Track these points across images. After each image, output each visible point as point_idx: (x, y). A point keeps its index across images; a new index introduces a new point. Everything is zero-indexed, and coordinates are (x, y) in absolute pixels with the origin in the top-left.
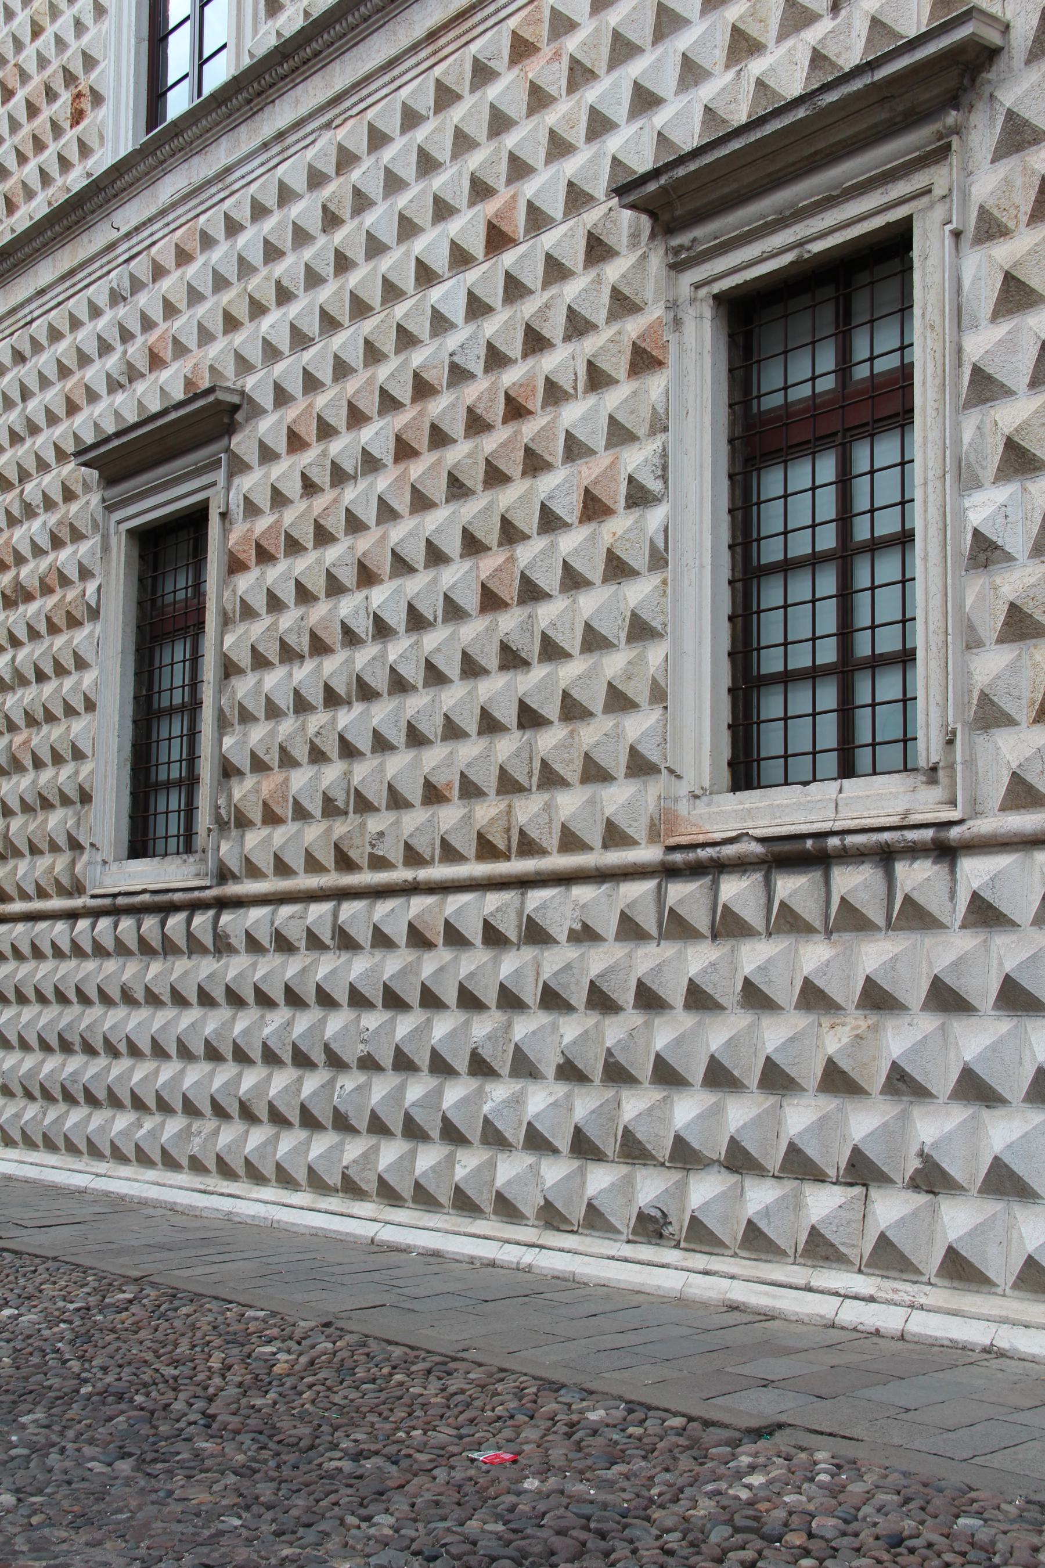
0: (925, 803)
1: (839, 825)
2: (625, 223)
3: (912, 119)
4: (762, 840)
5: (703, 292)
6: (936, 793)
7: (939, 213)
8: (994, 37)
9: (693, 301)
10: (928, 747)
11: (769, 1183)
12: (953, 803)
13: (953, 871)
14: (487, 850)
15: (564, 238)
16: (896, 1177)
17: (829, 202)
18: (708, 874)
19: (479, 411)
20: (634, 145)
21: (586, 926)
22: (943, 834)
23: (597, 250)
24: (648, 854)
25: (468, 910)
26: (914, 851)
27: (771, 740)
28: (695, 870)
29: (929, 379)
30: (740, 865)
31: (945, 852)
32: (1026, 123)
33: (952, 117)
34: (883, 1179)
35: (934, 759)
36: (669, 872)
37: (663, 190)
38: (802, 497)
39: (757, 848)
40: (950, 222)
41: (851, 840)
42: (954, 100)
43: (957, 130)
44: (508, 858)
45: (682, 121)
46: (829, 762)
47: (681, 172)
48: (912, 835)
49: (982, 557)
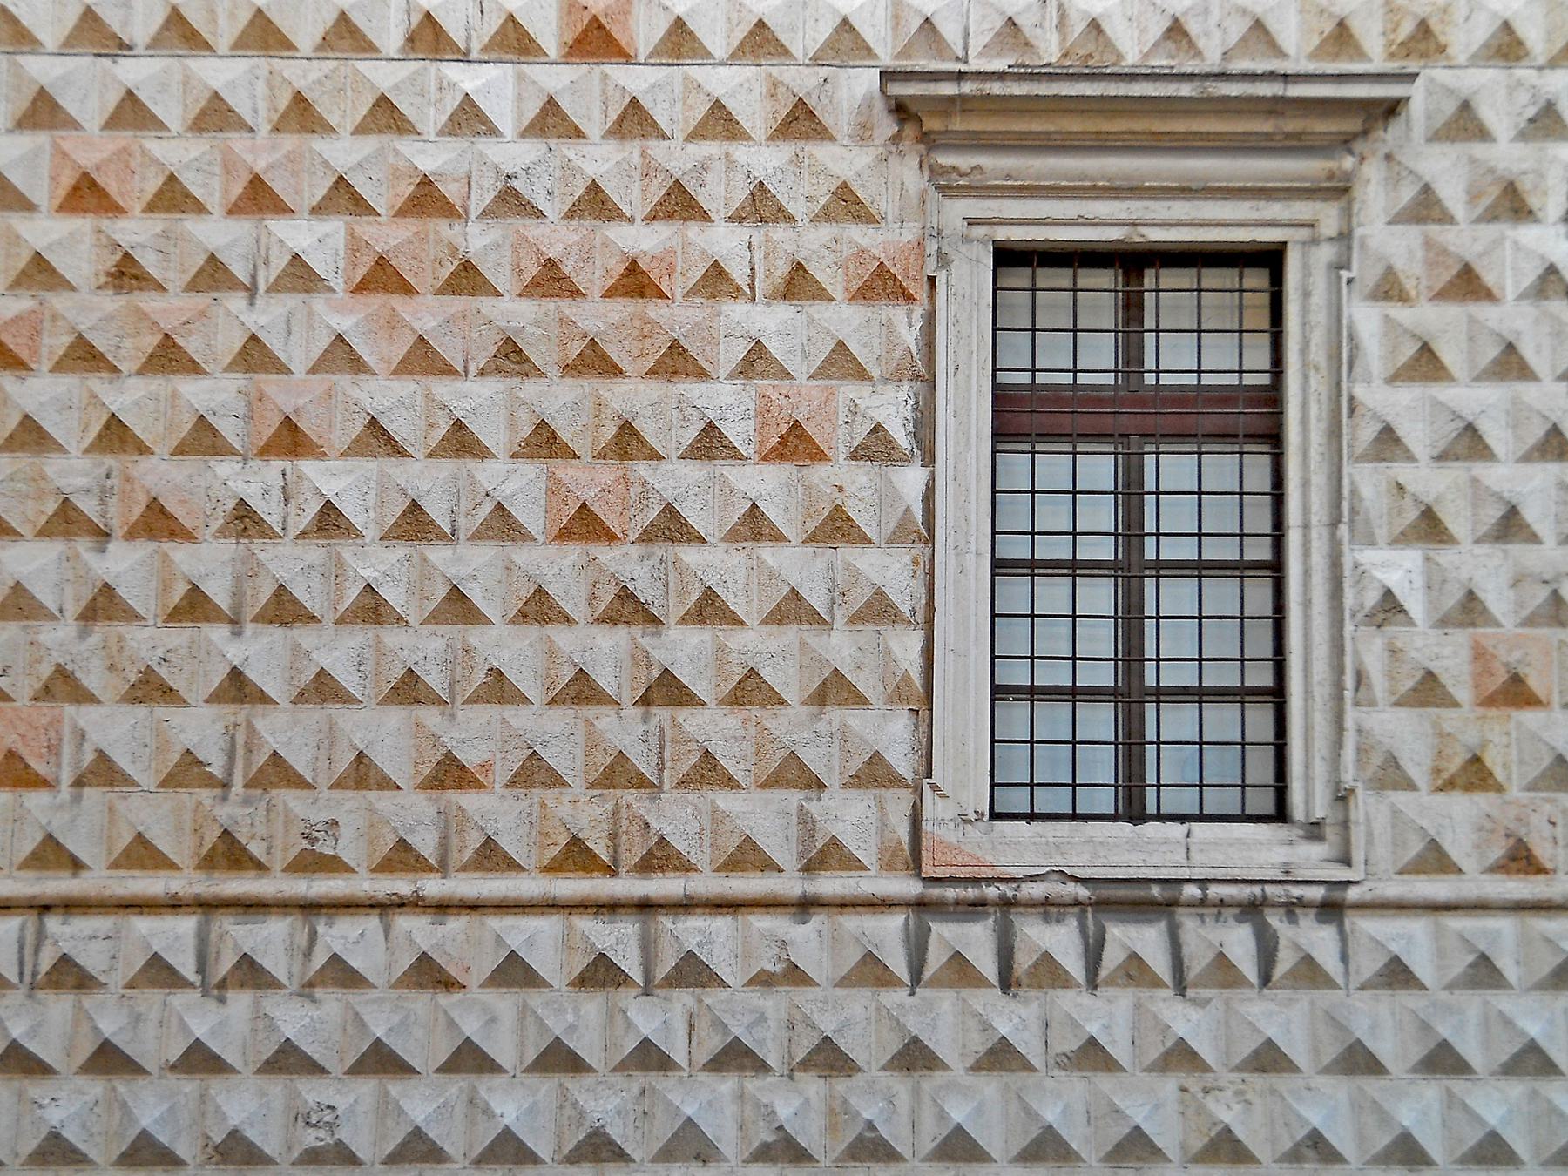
0: (1312, 859)
5: (980, 231)
6: (1316, 851)
9: (966, 239)
12: (1346, 861)
14: (576, 856)
18: (986, 915)
19: (566, 269)
22: (1337, 894)
23: (800, 122)
24: (910, 888)
25: (536, 938)
26: (1291, 908)
28: (976, 908)
29: (1313, 421)
30: (1048, 908)
31: (1331, 910)
32: (1438, 202)
33: (1348, 162)
35: (1319, 813)
39: (1083, 892)
40: (1348, 267)
42: (1346, 142)
44: (612, 871)
48: (1296, 891)
49: (1382, 616)
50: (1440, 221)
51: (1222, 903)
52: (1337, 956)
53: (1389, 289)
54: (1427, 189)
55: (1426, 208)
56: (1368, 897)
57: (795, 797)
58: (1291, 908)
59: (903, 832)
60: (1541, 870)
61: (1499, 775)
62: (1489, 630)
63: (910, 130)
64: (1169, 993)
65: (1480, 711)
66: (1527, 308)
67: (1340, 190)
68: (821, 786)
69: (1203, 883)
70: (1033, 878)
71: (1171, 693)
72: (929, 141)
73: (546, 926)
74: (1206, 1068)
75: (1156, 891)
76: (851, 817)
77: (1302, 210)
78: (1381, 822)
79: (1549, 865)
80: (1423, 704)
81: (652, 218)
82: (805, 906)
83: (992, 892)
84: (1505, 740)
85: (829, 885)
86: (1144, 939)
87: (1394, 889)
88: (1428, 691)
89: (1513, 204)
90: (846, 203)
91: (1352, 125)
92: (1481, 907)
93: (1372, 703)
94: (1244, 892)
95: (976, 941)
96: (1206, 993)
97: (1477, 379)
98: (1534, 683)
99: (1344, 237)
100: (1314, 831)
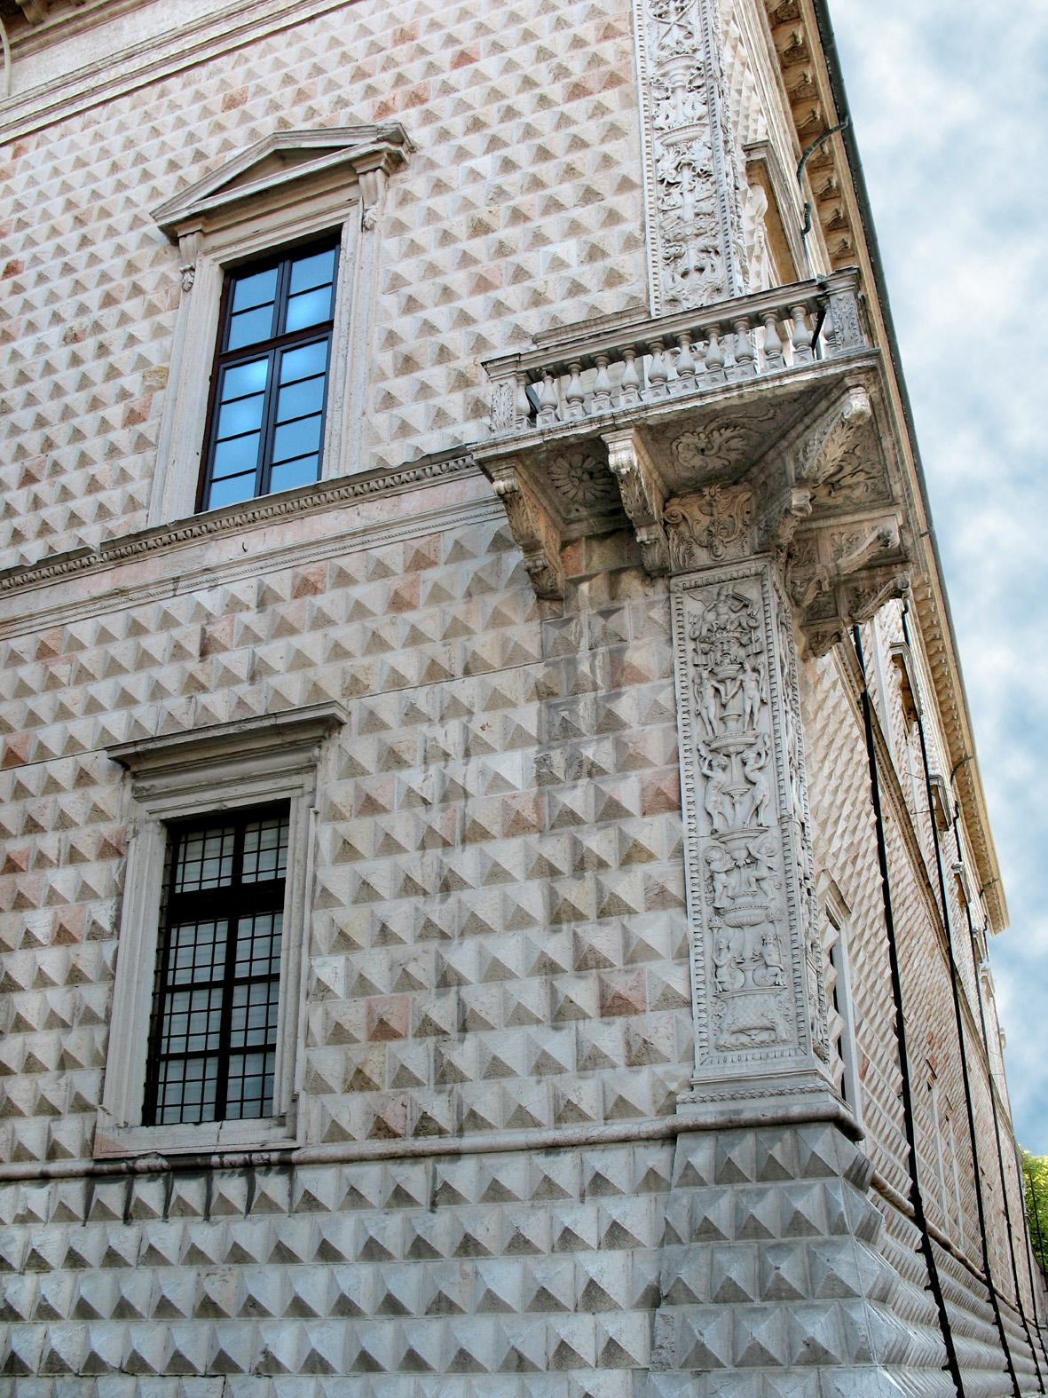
1: (219, 1150)
2: (100, 763)
3: (295, 747)
4: (166, 1157)
5: (155, 816)
6: (282, 1132)
7: (306, 800)
8: (342, 716)
9: (147, 822)
10: (280, 1103)
11: (157, 1379)
12: (294, 1137)
13: (292, 1180)
15: (63, 770)
16: (245, 1368)
17: (244, 780)
18: (122, 1179)
20: (118, 726)
21: (30, 1212)
22: (286, 1156)
23: (83, 778)
24: (83, 1165)
26: (268, 1165)
27: (172, 1095)
28: (115, 1176)
31: (286, 1165)
32: (359, 764)
33: (316, 752)
34: (236, 1369)
35: (283, 1110)
36: (92, 1177)
37: (137, 754)
38: (200, 947)
39: (165, 1163)
41: (227, 1158)
42: (318, 741)
43: (319, 759)
45: (150, 720)
46: (209, 1110)
47: (151, 746)
50: (363, 774)
51: (233, 1166)
52: (286, 1193)
53: (335, 815)
54: (351, 759)
55: (353, 769)
56: (302, 1157)
57: (47, 1119)
58: (268, 1165)
59: (88, 1136)
60: (396, 1135)
61: (376, 1079)
62: (377, 996)
63: (128, 773)
64: (200, 1219)
65: (371, 1043)
66: (405, 813)
67: (312, 767)
68: (60, 1113)
69: (222, 1154)
70: (144, 1156)
71: (210, 1045)
72: (135, 776)
73: (619, 1156)
74: (211, 1263)
75: (199, 1160)
76: (69, 1132)
77: (296, 780)
78: (315, 1114)
79: (400, 1132)
80: (341, 1043)
81: (24, 834)
82: (44, 1178)
83: (123, 1165)
84: (381, 1059)
85: (54, 1167)
86: (190, 1190)
87: (313, 1152)
88: (339, 1035)
89: (393, 759)
90: (97, 814)
91: (319, 733)
92: (362, 1159)
93: (315, 1045)
94: (239, 1158)
95: (111, 1195)
96: (219, 1218)
97: (377, 856)
98: (395, 1024)
99: (314, 791)
100: (281, 1121)
